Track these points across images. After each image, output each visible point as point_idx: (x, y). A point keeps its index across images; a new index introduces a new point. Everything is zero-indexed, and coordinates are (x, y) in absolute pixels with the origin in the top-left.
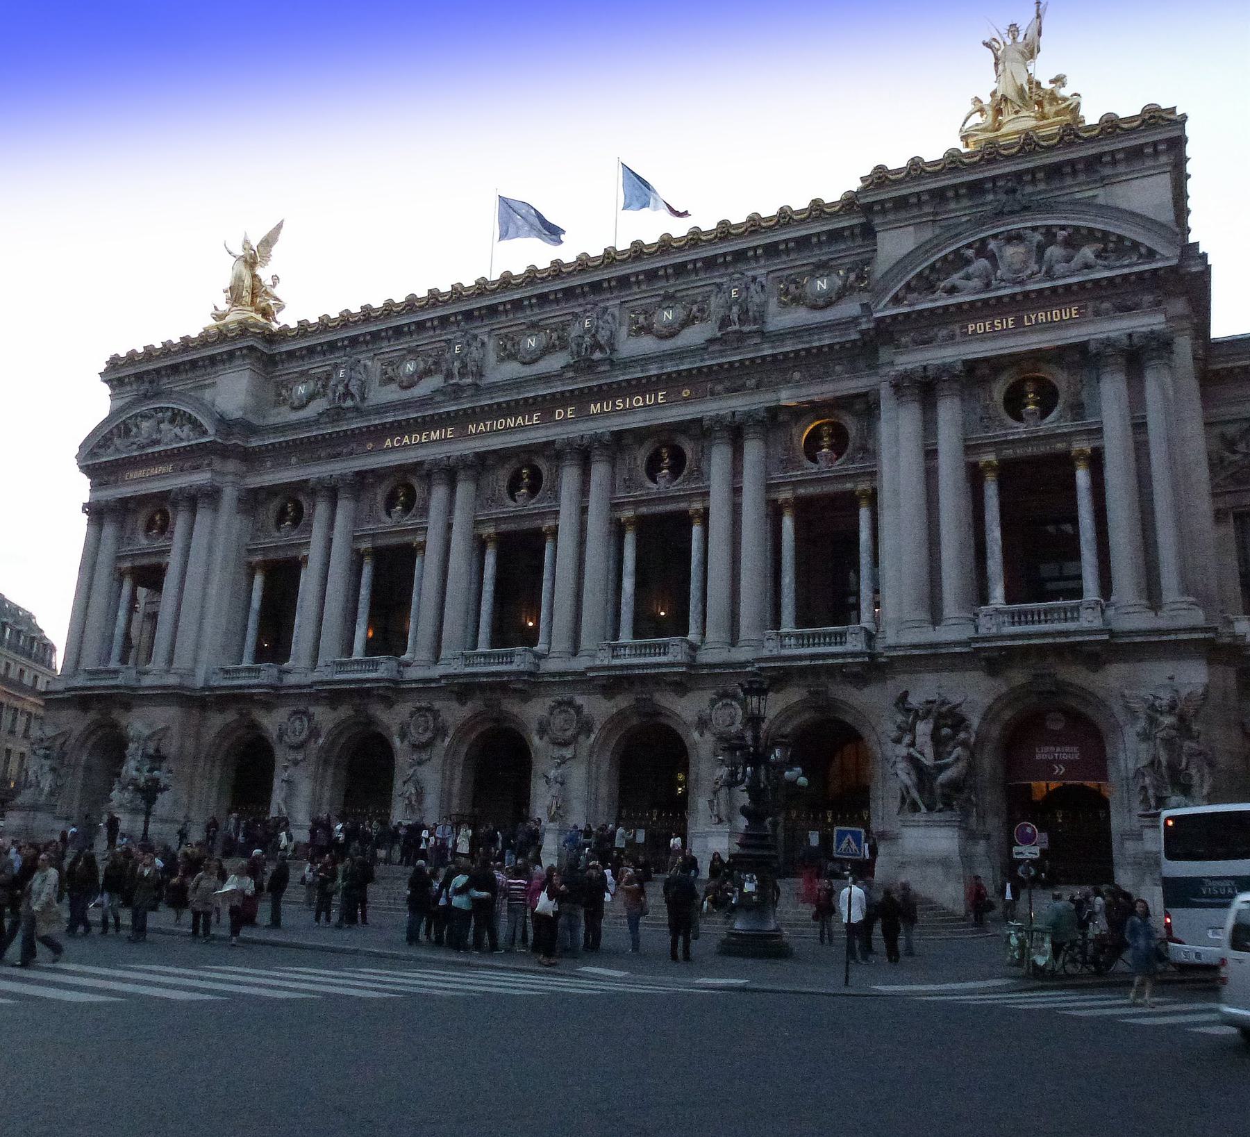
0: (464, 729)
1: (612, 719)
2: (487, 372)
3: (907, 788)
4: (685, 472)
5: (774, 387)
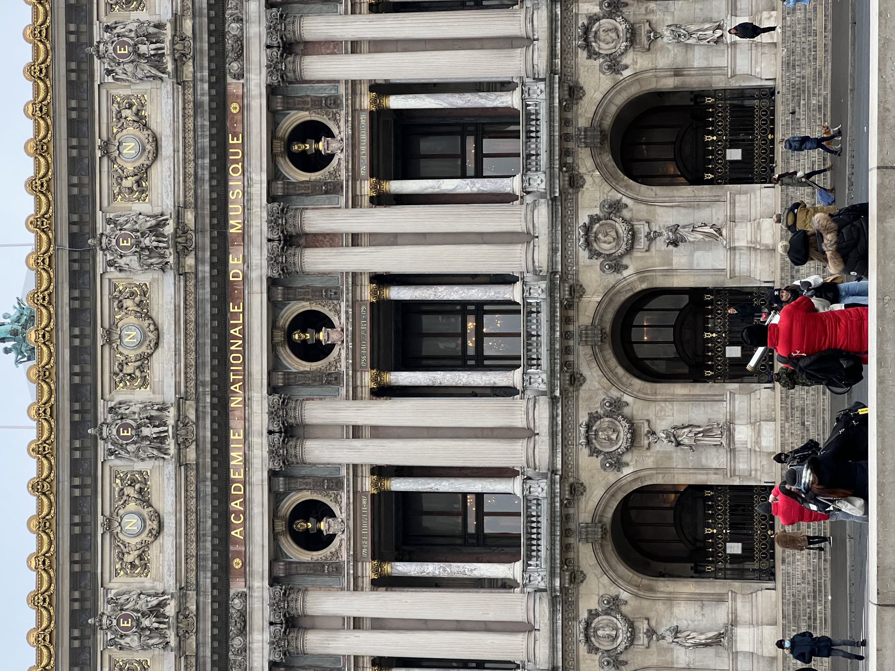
0: (614, 381)
1: (606, 179)
2: (158, 399)
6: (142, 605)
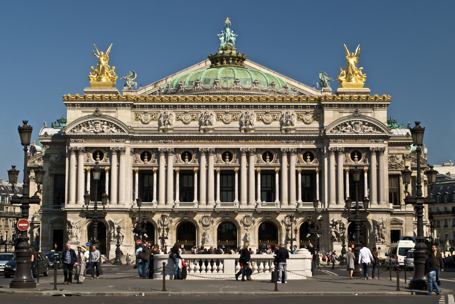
2: (214, 124)
3: (334, 237)
4: (273, 160)
5: (298, 144)
6: (170, 121)
